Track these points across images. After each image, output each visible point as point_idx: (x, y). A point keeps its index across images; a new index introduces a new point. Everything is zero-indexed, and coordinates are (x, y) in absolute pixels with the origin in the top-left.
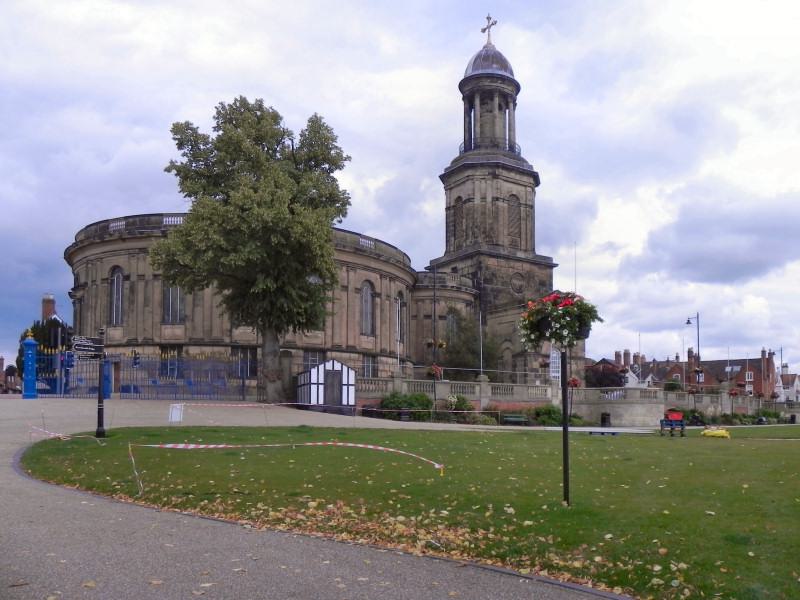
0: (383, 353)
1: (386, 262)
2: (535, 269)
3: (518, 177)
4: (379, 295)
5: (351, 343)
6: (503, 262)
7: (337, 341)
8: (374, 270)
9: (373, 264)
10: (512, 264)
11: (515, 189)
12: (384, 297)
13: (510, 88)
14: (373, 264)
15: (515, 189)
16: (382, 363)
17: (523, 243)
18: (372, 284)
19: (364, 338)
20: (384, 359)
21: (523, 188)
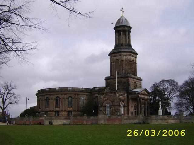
0: (62, 111)
1: (61, 91)
2: (122, 79)
3: (117, 54)
4: (61, 99)
5: (53, 110)
7: (50, 110)
8: (59, 94)
11: (117, 58)
13: (121, 28)
15: (117, 58)
16: (61, 113)
17: (120, 72)
18: (59, 97)
20: (61, 112)
21: (120, 56)
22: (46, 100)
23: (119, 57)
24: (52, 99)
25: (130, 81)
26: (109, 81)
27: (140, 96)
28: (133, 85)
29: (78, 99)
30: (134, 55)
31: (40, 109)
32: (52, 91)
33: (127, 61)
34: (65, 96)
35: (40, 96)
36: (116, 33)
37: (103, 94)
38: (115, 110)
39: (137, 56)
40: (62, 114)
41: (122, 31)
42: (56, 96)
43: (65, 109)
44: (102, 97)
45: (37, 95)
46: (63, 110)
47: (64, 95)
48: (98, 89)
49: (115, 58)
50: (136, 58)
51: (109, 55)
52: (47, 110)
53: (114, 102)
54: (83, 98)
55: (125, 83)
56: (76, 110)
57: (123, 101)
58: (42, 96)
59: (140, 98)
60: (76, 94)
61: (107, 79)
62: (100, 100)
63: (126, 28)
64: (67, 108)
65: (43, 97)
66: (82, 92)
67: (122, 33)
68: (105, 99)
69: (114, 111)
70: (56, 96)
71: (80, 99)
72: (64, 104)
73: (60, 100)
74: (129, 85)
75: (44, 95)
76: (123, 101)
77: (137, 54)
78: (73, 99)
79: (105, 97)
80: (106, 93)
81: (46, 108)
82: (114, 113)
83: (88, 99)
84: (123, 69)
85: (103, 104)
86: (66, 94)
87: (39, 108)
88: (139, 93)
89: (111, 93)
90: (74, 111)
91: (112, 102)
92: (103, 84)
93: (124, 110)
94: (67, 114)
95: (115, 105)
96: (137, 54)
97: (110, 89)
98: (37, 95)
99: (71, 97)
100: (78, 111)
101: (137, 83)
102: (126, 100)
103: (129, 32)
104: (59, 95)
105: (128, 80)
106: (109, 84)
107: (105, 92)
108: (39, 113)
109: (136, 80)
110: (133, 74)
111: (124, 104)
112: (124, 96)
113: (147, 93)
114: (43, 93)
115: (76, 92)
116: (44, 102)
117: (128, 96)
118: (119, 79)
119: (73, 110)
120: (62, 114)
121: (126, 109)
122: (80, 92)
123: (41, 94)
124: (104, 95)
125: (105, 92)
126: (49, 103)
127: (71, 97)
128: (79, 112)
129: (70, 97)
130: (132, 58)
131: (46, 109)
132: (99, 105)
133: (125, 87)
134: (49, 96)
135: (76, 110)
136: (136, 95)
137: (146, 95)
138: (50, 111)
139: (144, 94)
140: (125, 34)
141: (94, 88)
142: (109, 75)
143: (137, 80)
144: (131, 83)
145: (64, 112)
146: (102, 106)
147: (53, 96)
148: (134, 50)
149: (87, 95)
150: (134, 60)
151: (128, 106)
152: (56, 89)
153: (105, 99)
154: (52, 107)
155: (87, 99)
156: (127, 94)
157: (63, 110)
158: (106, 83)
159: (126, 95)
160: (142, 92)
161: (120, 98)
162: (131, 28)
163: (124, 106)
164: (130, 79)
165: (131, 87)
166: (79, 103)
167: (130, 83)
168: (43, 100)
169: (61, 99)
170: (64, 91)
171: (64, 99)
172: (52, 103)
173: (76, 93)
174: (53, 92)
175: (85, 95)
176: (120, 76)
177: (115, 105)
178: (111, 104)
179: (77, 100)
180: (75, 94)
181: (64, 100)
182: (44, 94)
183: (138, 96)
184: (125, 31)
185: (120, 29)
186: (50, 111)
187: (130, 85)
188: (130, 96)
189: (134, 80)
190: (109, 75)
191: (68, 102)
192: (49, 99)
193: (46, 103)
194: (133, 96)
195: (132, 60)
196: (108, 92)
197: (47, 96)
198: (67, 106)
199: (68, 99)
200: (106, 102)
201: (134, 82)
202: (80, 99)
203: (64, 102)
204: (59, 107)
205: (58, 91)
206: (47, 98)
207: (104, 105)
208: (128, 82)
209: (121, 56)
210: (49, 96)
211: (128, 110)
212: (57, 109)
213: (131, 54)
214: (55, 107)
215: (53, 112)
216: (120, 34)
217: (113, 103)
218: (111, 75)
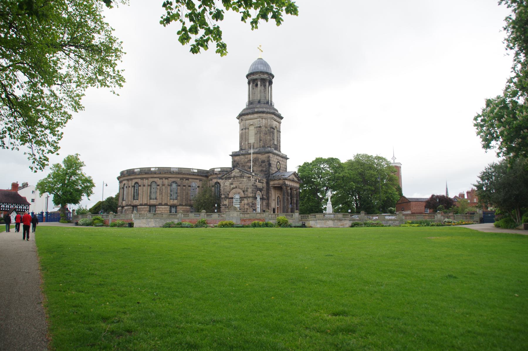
0: (160, 204)
1: (160, 174)
2: (260, 156)
4: (159, 185)
5: (146, 203)
6: (242, 157)
7: (141, 203)
8: (155, 178)
9: (155, 176)
10: (247, 156)
12: (161, 186)
13: (258, 76)
14: (155, 176)
15: (251, 122)
16: (159, 208)
18: (156, 183)
19: (151, 201)
20: (160, 207)
22: (134, 187)
23: (254, 121)
24: (144, 186)
25: (272, 159)
26: (237, 158)
27: (287, 182)
28: (275, 166)
29: (187, 186)
30: (278, 119)
31: (124, 202)
32: (146, 172)
33: (266, 127)
34: (166, 180)
35: (124, 180)
36: (249, 83)
37: (230, 178)
38: (248, 204)
39: (282, 121)
40: (160, 209)
41: (260, 79)
42: (151, 180)
43: (166, 202)
44: (228, 183)
45: (118, 178)
46: (163, 204)
47: (164, 179)
48: (220, 171)
49: (247, 122)
50: (280, 123)
51: (238, 118)
52: (136, 202)
53: (247, 191)
54: (195, 184)
55: (263, 162)
56: (184, 204)
57: (261, 190)
58: (128, 180)
59: (287, 186)
60: (185, 178)
61: (234, 155)
62: (224, 189)
63: (265, 76)
64: (169, 200)
65: (130, 182)
66: (194, 175)
67: (259, 83)
68: (232, 186)
69: (246, 207)
70: (151, 180)
71: (190, 186)
72: (163, 194)
73: (158, 187)
74: (270, 165)
75: (131, 179)
76: (261, 190)
77: (282, 118)
78: (179, 186)
79: (232, 184)
80: (234, 177)
81: (134, 199)
82: (247, 209)
83: (202, 187)
84: (260, 140)
85: (228, 195)
86: (167, 178)
87: (123, 200)
88: (286, 179)
89: (242, 176)
90: (181, 205)
91: (244, 192)
92: (228, 164)
93: (262, 205)
94: (168, 209)
95: (249, 197)
96: (282, 118)
97: (240, 171)
98: (118, 178)
99: (176, 183)
100: (186, 205)
101: (281, 162)
102: (265, 189)
103: (271, 83)
104: (155, 180)
105: (269, 157)
106: (238, 164)
107: (233, 175)
108: (123, 207)
109: (280, 158)
110: (276, 149)
111: (262, 195)
112: (262, 183)
113: (296, 179)
114: (129, 175)
115: (184, 174)
116: (131, 190)
117: (268, 183)
118: (255, 155)
119: (179, 204)
120: (160, 209)
121: (264, 204)
122: (190, 174)
123: (126, 176)
124: (230, 181)
125: (233, 175)
126: (140, 192)
127: (176, 183)
128: (188, 207)
129: (173, 182)
130: (275, 124)
131: (135, 201)
132: (223, 196)
133: (264, 169)
134: (139, 181)
135: (184, 204)
136: (281, 182)
137: (296, 182)
138: (141, 205)
139: (293, 181)
140: (265, 86)
141: (213, 170)
142: (237, 149)
143: (282, 159)
144: (273, 163)
145: (163, 207)
146: (227, 198)
147: (147, 181)
148: (277, 111)
149: (200, 180)
150: (278, 127)
151: (268, 199)
152: (152, 169)
153: (232, 186)
154: (143, 199)
155: (201, 186)
156: (267, 180)
157: (163, 204)
158: (234, 162)
159: (265, 180)
160: (290, 177)
161: (256, 186)
162: (273, 77)
163: (262, 199)
164: (271, 155)
165: (273, 169)
166: (189, 192)
167: (271, 162)
168: (129, 187)
169: (159, 185)
170: (165, 173)
171: (163, 185)
172: (144, 191)
173: (185, 176)
174: (146, 173)
175: (198, 181)
176: (256, 150)
177: (249, 197)
178: (243, 195)
179: (184, 188)
180: (182, 179)
181: (164, 187)
182: (132, 177)
183: (285, 184)
184: (263, 81)
185: (255, 77)
186: (141, 205)
187: (272, 165)
188: (271, 183)
189: (278, 157)
190: (237, 149)
191: (171, 191)
192: (140, 186)
193: (134, 192)
194: (276, 182)
195: (274, 126)
196: (237, 175)
197: (136, 180)
198: (169, 198)
199: (171, 185)
200: (234, 191)
201: (276, 161)
202: (190, 186)
203: (164, 191)
204: (156, 199)
205: (155, 173)
206: (136, 183)
207: (230, 196)
208: (269, 161)
209: (258, 119)
210: (139, 181)
211: (268, 205)
212: (153, 202)
213: (273, 116)
214: (149, 198)
215: (145, 207)
216: (257, 85)
217: (246, 193)
218: (241, 149)
